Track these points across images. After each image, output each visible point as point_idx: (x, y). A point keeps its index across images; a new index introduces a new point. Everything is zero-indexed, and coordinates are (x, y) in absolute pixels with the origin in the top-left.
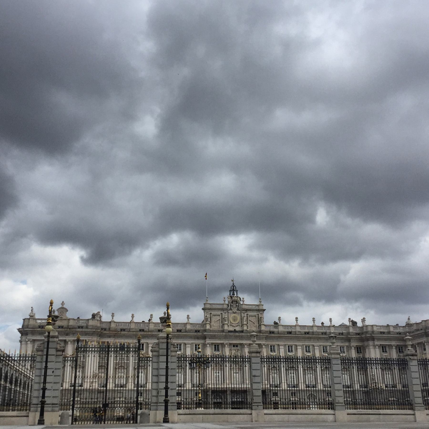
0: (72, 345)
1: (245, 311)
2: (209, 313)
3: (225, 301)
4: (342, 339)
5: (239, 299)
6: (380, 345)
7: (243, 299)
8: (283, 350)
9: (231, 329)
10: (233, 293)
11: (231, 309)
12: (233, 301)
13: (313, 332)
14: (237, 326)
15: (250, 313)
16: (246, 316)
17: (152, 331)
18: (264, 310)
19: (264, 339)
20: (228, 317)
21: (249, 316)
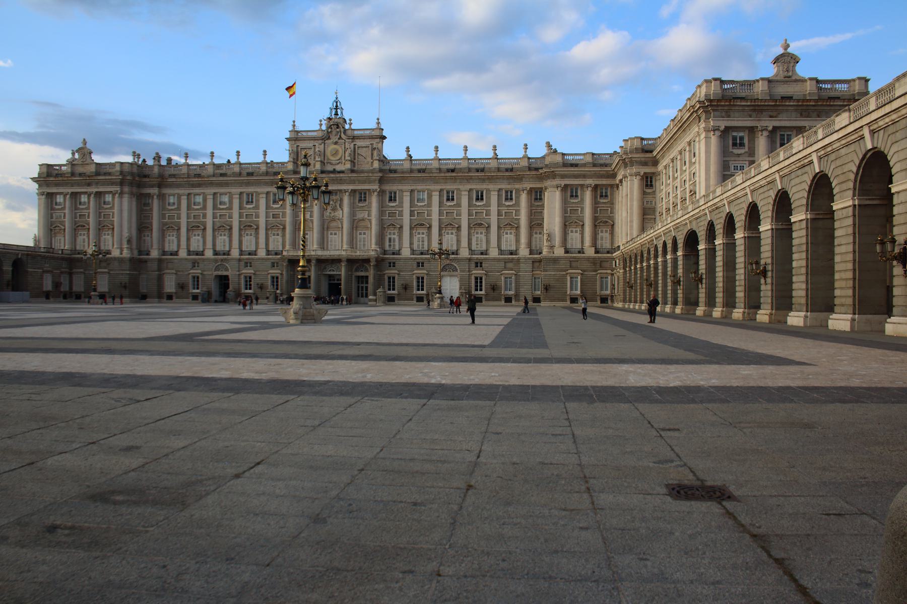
0: (98, 199)
1: (351, 140)
2: (295, 146)
3: (321, 125)
4: (510, 178)
5: (341, 121)
6: (566, 186)
7: (350, 120)
8: (408, 198)
9: (329, 168)
10: (337, 112)
11: (329, 138)
12: (331, 125)
13: (461, 168)
14: (338, 164)
15: (359, 143)
16: (352, 146)
17: (208, 177)
18: (385, 138)
19: (377, 182)
20: (324, 150)
21: (358, 147)
